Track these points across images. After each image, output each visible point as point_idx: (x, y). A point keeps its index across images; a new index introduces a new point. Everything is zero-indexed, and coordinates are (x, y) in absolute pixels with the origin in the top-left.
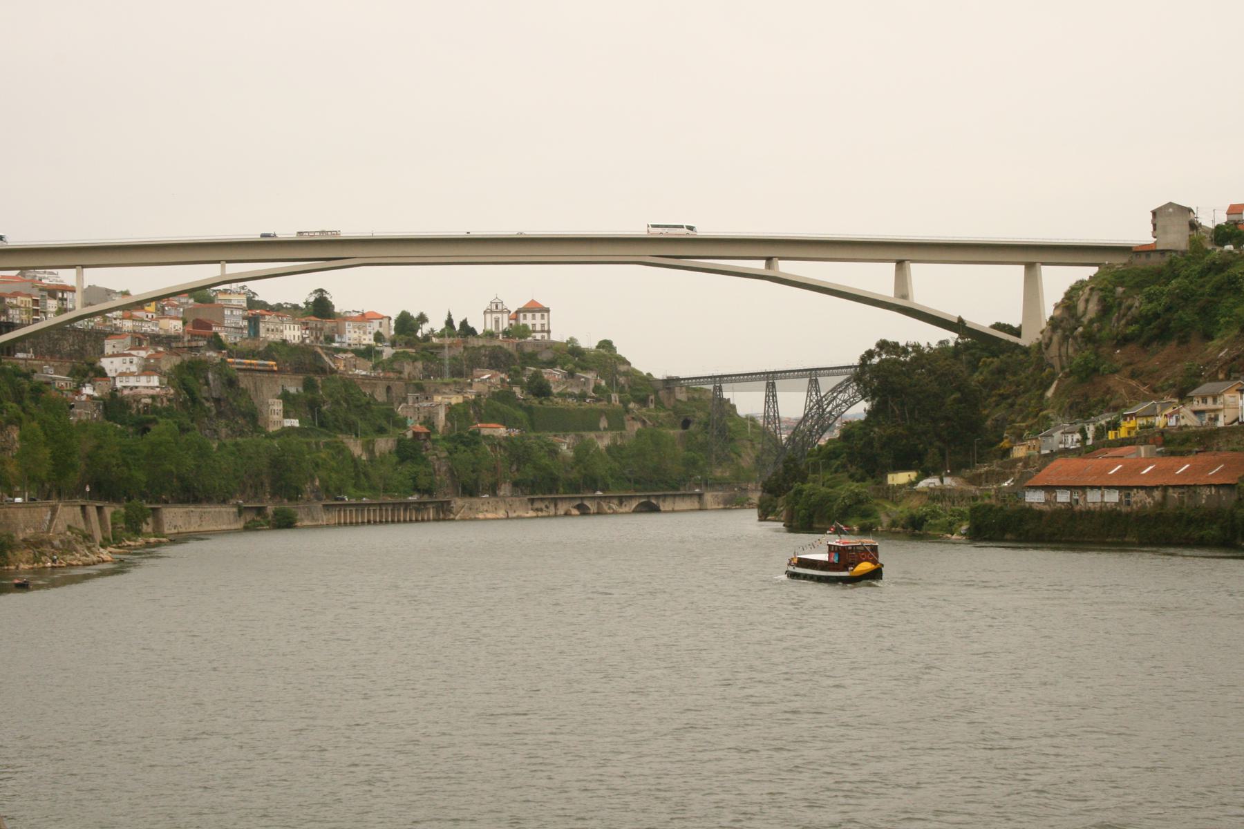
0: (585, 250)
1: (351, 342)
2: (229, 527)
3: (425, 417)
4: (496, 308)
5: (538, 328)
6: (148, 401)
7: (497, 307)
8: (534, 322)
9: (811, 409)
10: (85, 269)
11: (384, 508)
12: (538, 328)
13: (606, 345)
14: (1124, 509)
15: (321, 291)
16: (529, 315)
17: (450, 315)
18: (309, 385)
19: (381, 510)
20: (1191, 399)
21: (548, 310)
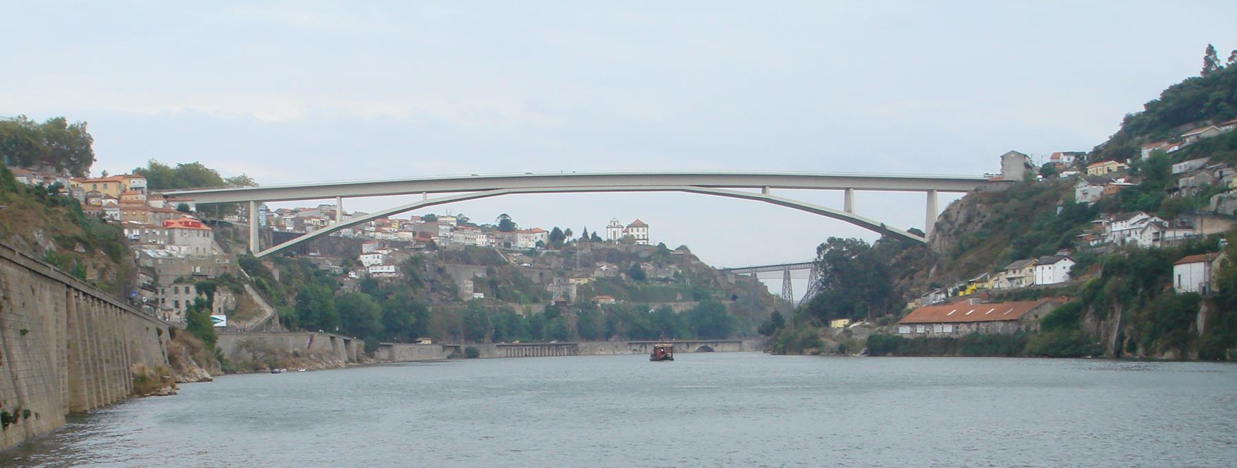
2: (437, 358)
4: (614, 225)
6: (389, 281)
7: (614, 224)
9: (812, 288)
11: (535, 348)
12: (641, 237)
13: (661, 243)
14: (954, 336)
15: (505, 215)
16: (635, 229)
17: (585, 230)
18: (489, 272)
19: (533, 349)
20: (1007, 271)
21: (647, 226)
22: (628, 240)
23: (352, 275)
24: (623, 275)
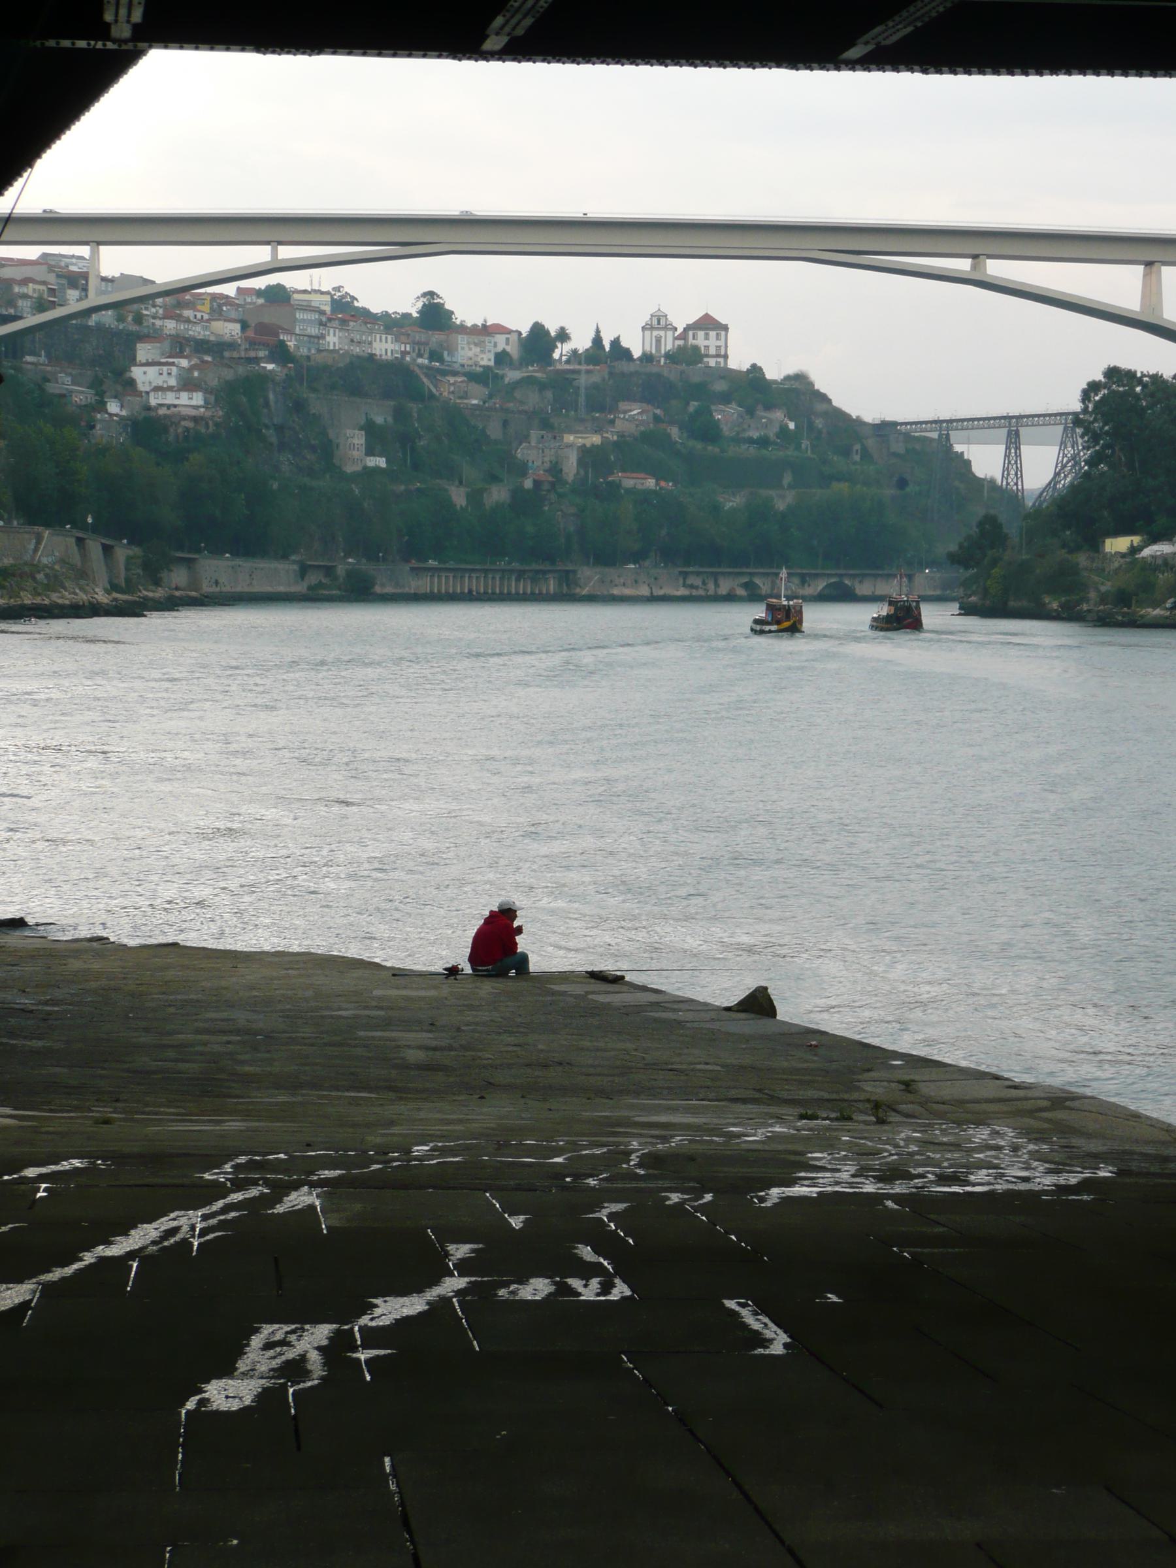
0: (735, 240)
1: (464, 362)
3: (551, 462)
4: (658, 323)
5: (712, 351)
7: (659, 323)
8: (707, 343)
9: (1064, 466)
10: (101, 247)
11: (490, 576)
12: (712, 351)
13: (754, 366)
15: (431, 294)
16: (701, 334)
17: (598, 331)
18: (400, 414)
21: (725, 328)
22: (687, 355)
23: (113, 407)
24: (674, 432)
